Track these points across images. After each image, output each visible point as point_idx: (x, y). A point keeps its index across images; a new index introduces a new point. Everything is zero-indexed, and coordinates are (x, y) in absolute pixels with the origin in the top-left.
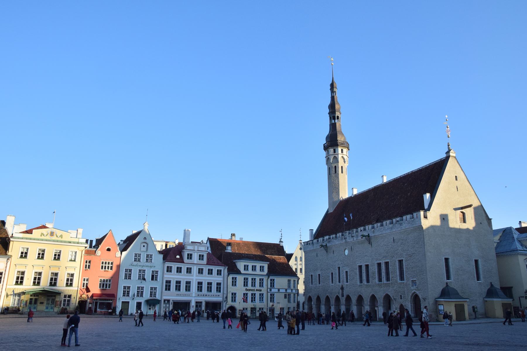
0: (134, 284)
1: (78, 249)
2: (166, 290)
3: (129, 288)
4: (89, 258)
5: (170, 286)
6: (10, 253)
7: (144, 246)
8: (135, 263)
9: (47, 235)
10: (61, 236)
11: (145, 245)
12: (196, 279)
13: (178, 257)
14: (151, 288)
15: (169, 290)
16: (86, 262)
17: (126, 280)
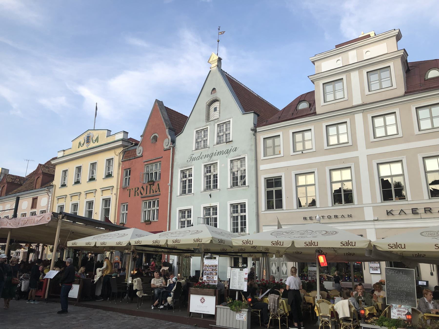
0: (197, 202)
1: (115, 153)
2: (270, 206)
3: (189, 211)
4: (127, 164)
5: (279, 194)
6: (54, 183)
7: (215, 109)
8: (197, 154)
9: (83, 145)
10: (97, 140)
11: (216, 104)
12: (370, 157)
13: (303, 106)
14: (234, 207)
15: (279, 205)
16: (127, 175)
17: (184, 196)
